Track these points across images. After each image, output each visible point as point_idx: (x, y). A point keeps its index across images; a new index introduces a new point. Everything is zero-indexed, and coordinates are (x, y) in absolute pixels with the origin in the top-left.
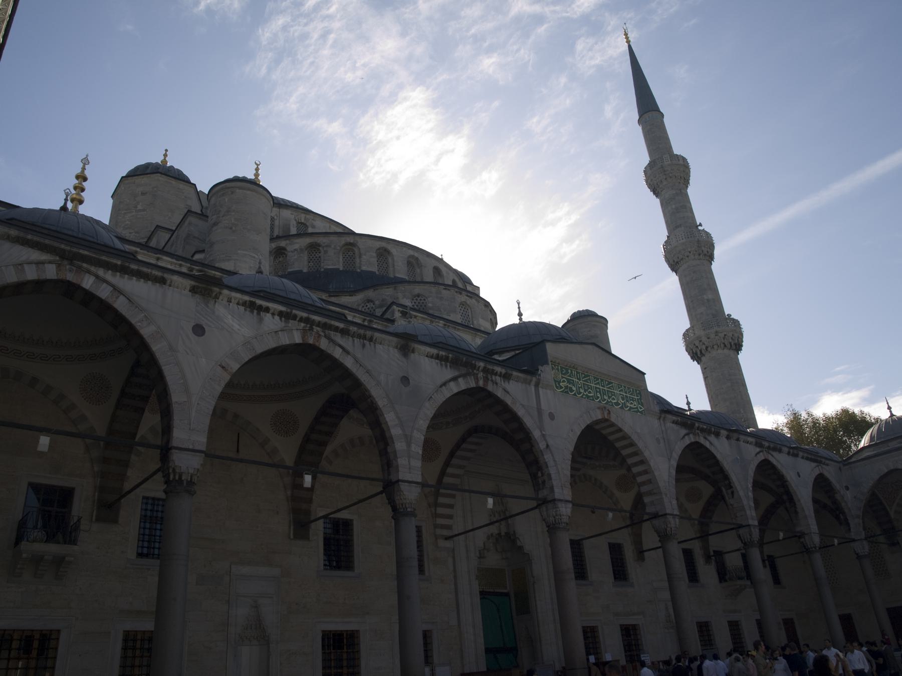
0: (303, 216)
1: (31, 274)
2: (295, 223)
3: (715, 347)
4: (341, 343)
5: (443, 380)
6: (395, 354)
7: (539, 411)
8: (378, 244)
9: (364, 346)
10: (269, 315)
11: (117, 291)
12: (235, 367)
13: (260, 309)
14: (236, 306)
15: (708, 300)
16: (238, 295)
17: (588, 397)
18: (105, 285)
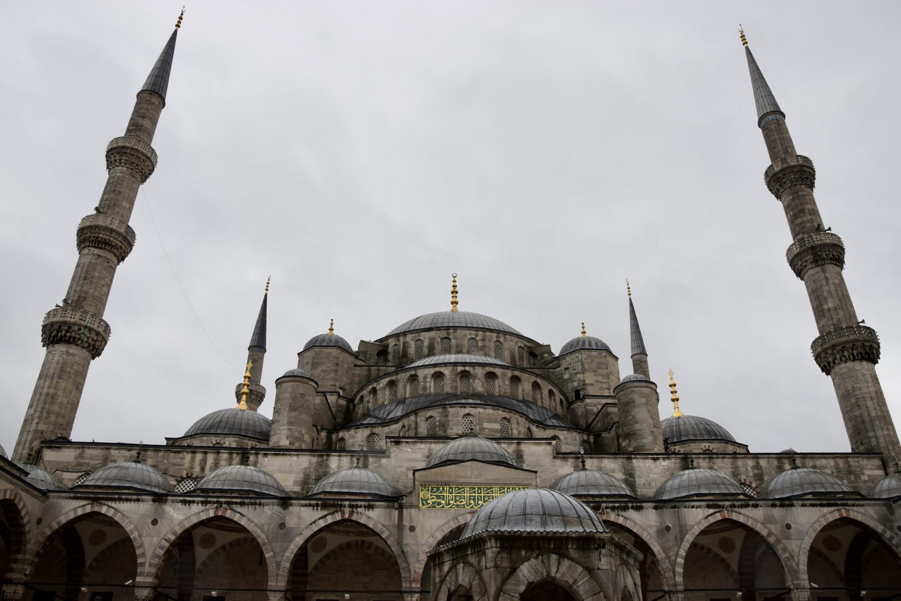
1: (80, 512)
3: (836, 361)
5: (313, 520)
6: (277, 509)
7: (400, 527)
8: (433, 371)
12: (173, 538)
15: (829, 310)
17: (458, 506)
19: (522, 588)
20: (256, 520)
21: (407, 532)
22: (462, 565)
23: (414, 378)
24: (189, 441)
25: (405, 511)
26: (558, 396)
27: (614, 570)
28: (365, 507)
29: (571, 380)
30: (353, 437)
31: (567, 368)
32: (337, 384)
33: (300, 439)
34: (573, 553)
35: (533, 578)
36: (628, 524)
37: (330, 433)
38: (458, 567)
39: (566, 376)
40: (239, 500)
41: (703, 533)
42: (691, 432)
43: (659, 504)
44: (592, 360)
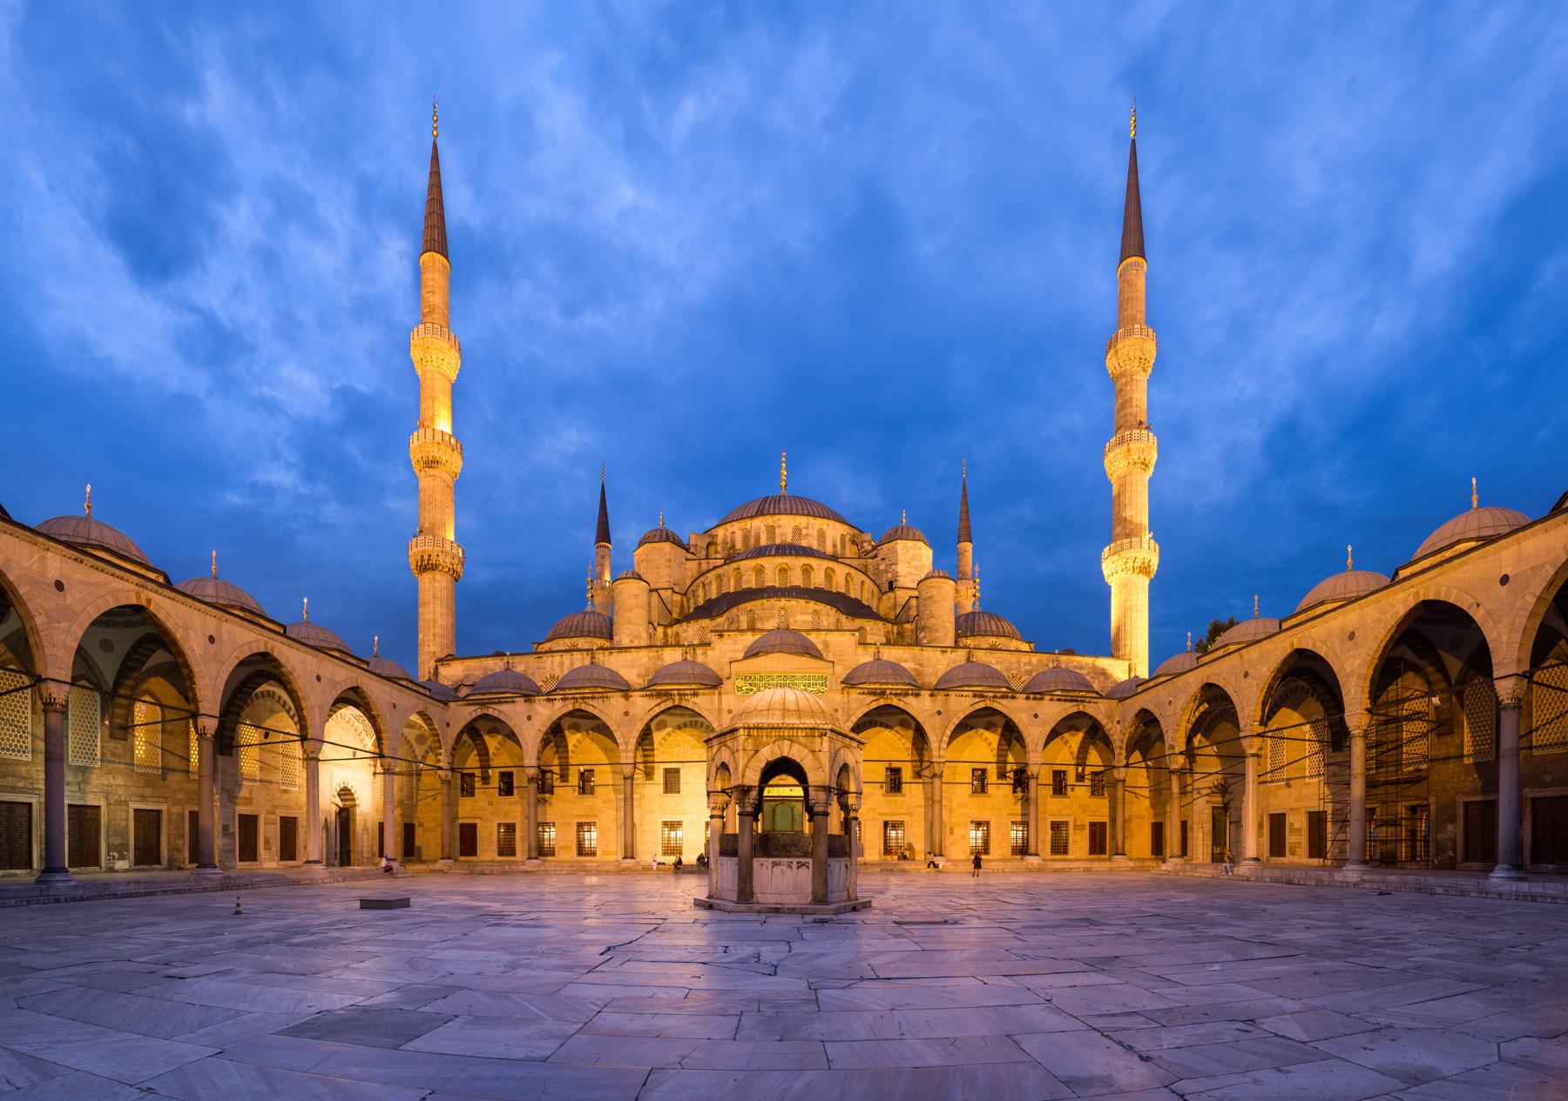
7: (720, 710)
26: (869, 584)
33: (638, 637)
36: (906, 708)
37: (666, 627)
39: (882, 567)
41: (967, 717)
43: (934, 690)
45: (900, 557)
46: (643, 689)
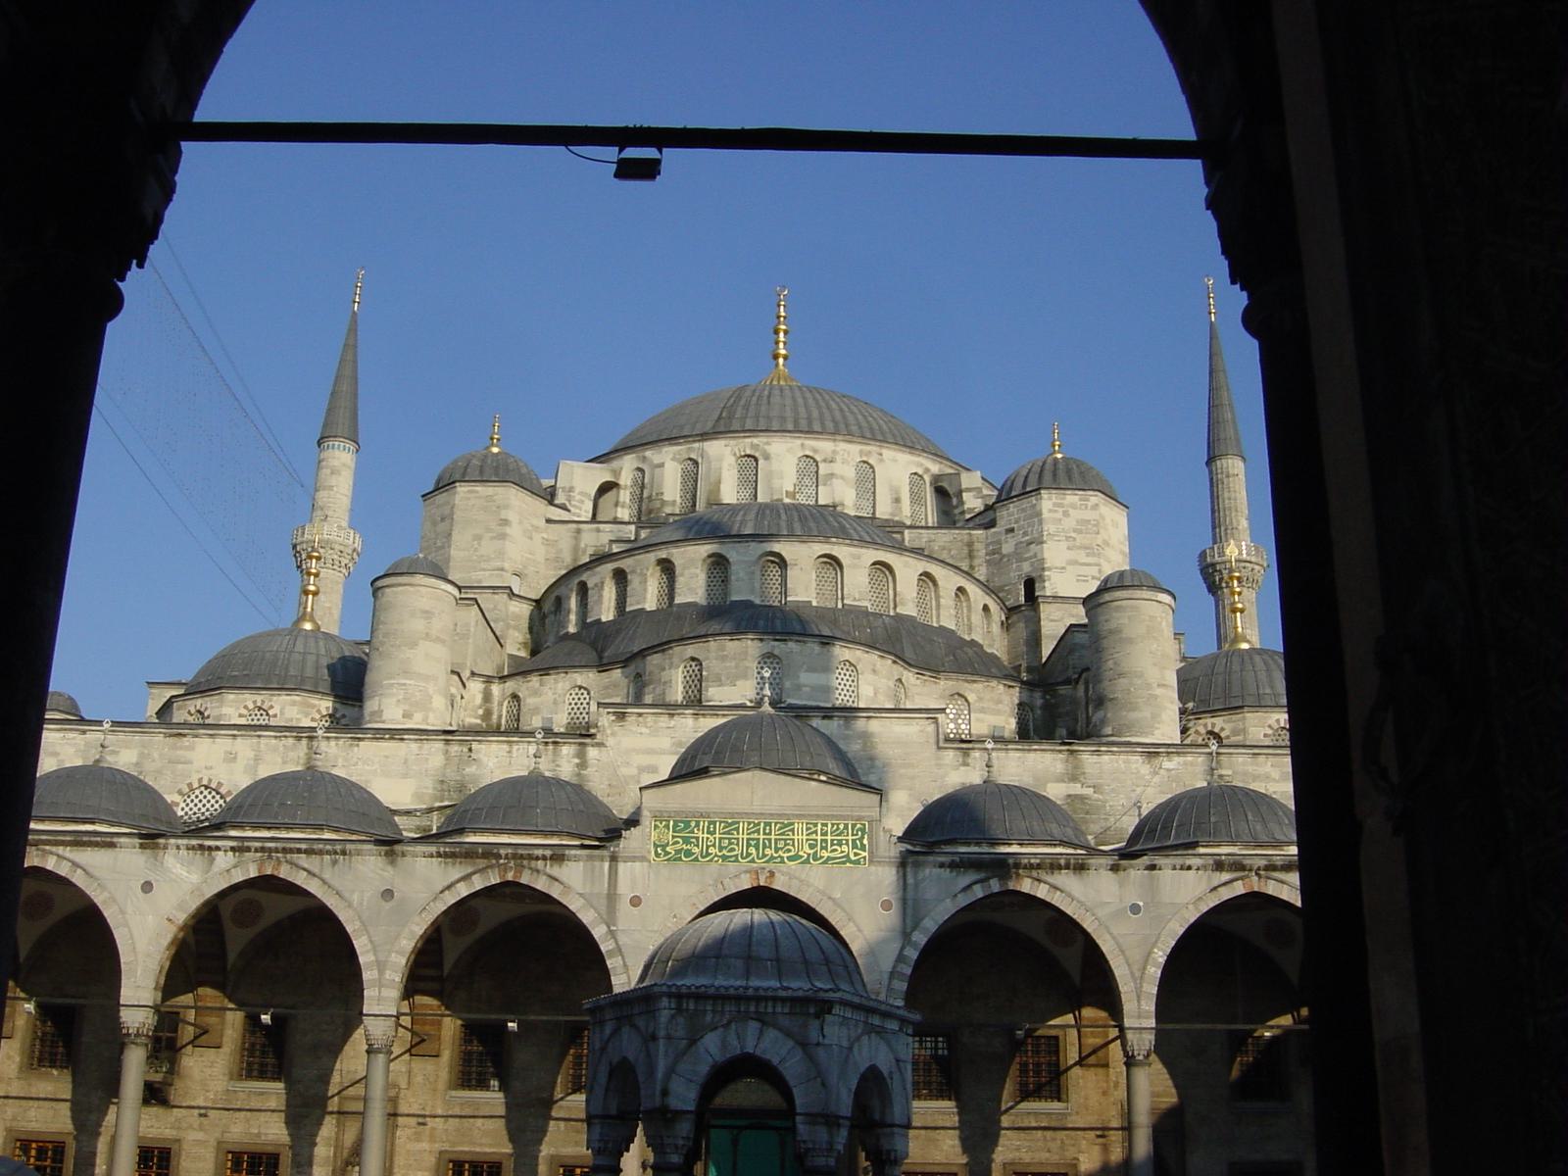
0: (747, 440)
2: (733, 459)
4: (306, 866)
5: (446, 884)
7: (612, 897)
9: (335, 862)
10: (221, 853)
11: (75, 865)
12: (181, 917)
13: (210, 848)
14: (185, 852)
16: (185, 842)
17: (725, 858)
18: (65, 861)
19: (704, 1069)
20: (335, 883)
21: (624, 906)
22: (628, 1027)
23: (667, 567)
24: (199, 702)
25: (622, 867)
27: (845, 1044)
28: (544, 858)
29: (1018, 555)
30: (536, 693)
31: (1012, 530)
32: (506, 565)
34: (784, 1021)
35: (719, 1058)
36: (1057, 900)
38: (623, 1029)
40: (303, 846)
42: (1252, 690)
44: (1066, 514)
45: (1049, 528)
46: (426, 838)
